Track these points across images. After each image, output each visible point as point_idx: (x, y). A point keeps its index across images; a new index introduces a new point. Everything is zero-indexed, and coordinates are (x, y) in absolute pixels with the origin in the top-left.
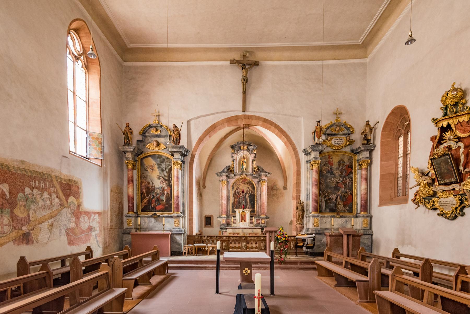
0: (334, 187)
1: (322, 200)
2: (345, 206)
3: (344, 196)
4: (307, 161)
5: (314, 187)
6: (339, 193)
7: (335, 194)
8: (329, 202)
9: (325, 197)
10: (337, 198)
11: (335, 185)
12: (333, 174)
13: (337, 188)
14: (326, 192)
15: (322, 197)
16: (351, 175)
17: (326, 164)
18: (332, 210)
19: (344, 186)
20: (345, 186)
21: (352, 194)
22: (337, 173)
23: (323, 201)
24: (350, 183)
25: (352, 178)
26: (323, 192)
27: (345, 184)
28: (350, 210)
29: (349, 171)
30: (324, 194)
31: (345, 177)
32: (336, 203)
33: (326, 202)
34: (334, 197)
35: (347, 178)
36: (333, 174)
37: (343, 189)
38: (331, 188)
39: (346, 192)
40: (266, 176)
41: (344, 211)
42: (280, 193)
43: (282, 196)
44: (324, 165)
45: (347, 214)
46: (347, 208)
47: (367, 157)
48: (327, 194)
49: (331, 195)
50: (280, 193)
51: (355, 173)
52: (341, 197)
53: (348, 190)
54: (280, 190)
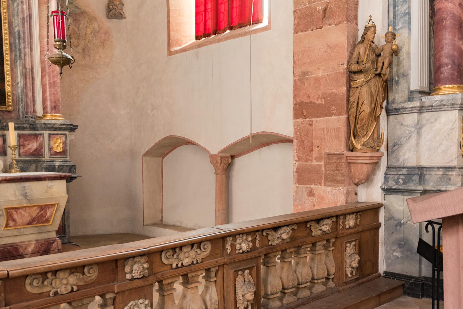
42: (95, 33)
43: (103, 43)
50: (95, 33)
54: (93, 19)
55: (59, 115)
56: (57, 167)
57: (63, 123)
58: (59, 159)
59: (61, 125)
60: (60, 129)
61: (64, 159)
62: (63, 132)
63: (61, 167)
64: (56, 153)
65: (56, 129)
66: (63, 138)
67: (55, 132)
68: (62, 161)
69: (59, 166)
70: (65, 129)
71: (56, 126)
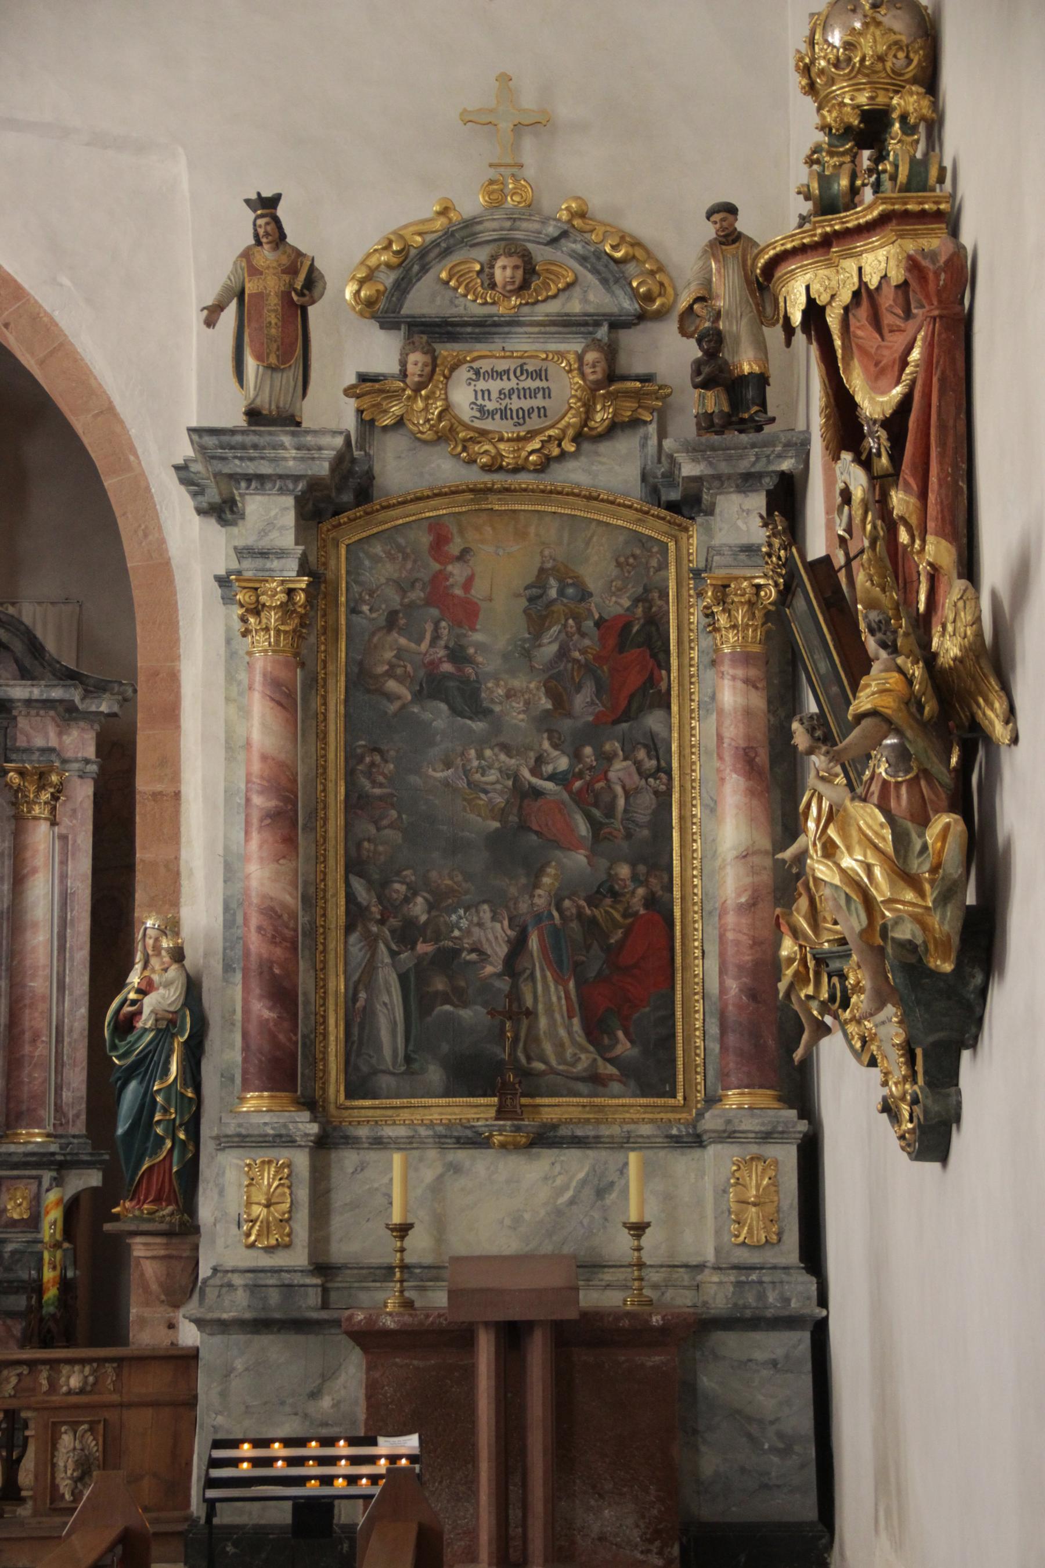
0: (494, 840)
1: (371, 967)
2: (596, 1030)
3: (590, 925)
4: (223, 581)
5: (255, 838)
6: (541, 899)
7: (499, 902)
8: (439, 984)
9: (407, 934)
10: (518, 946)
11: (502, 814)
12: (479, 711)
13: (517, 840)
14: (413, 891)
15: (371, 942)
16: (653, 721)
17: (411, 606)
18: (470, 1075)
19: (583, 828)
20: (595, 826)
21: (660, 908)
22: (517, 698)
23: (388, 977)
24: (647, 801)
25: (657, 747)
26: (380, 888)
27: (593, 799)
28: (654, 1071)
29: (634, 680)
30: (389, 908)
31: (592, 734)
32: (515, 995)
33: (414, 987)
34: (494, 936)
35: (612, 746)
36: (479, 711)
37: (580, 858)
38: (456, 847)
39: (608, 890)
40: (69, 713)
41: (595, 1080)
44: (392, 622)
45: (629, 1109)
46: (624, 1047)
47: (750, 549)
48: (419, 909)
49: (460, 919)
51: (685, 696)
52: (556, 939)
53: (624, 871)
55: (37, 1131)
56: (6, 1256)
57: (36, 1150)
58: (20, 1235)
59: (26, 1155)
60: (26, 1165)
61: (34, 1235)
62: (34, 1172)
63: (17, 1257)
64: (13, 1223)
65: (16, 1166)
66: (34, 1187)
67: (15, 1173)
68: (27, 1242)
69: (13, 1253)
70: (38, 1165)
71: (15, 1159)
